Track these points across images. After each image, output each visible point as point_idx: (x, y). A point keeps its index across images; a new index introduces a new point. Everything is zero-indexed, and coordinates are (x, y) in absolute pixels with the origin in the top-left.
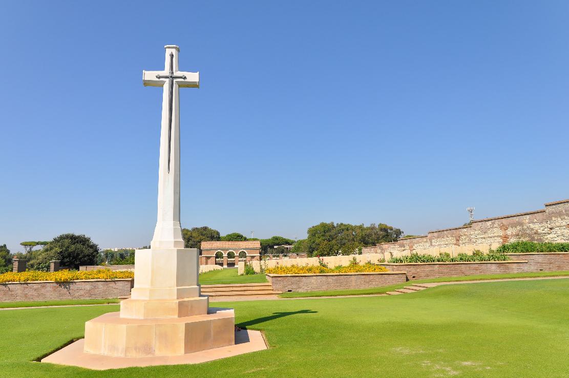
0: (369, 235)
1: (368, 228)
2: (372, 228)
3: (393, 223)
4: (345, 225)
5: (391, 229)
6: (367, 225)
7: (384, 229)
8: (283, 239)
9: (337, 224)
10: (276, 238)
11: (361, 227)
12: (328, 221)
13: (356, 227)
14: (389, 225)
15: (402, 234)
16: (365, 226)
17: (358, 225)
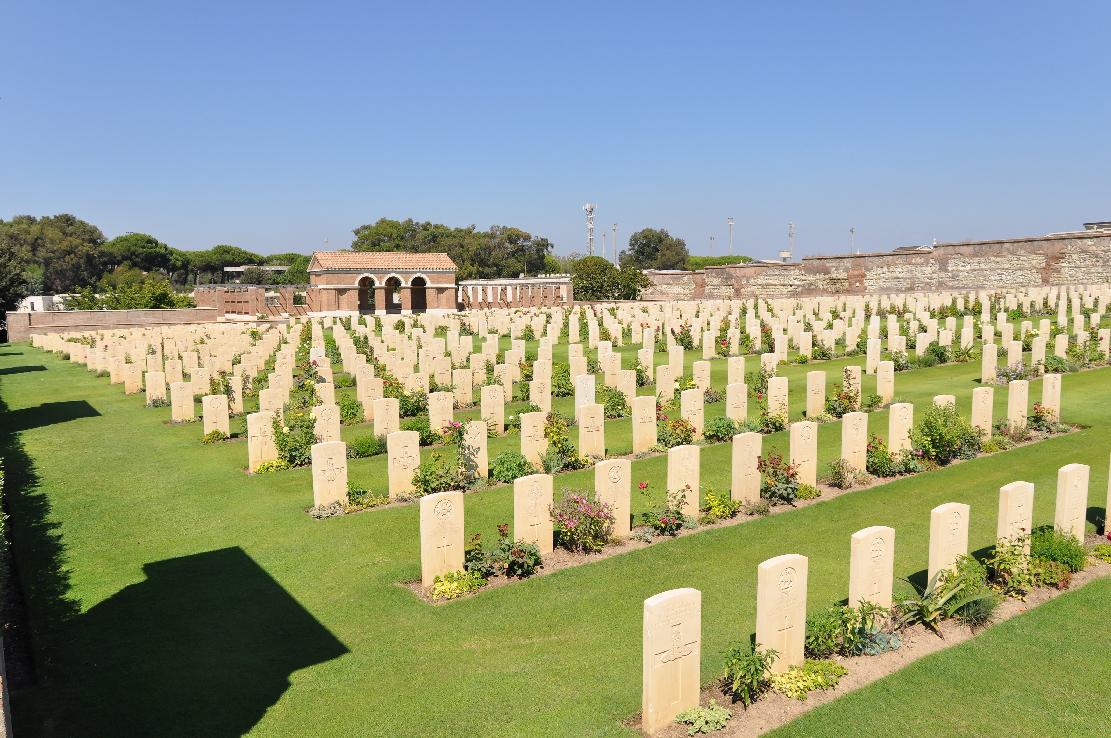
0: (489, 249)
1: (486, 235)
2: (492, 236)
3: (534, 228)
4: (436, 227)
5: (527, 238)
6: (482, 228)
7: (513, 237)
8: (240, 252)
9: (417, 223)
10: (225, 250)
11: (469, 232)
12: (401, 220)
13: (459, 231)
14: (524, 229)
15: (549, 248)
16: (475, 231)
17: (464, 227)
